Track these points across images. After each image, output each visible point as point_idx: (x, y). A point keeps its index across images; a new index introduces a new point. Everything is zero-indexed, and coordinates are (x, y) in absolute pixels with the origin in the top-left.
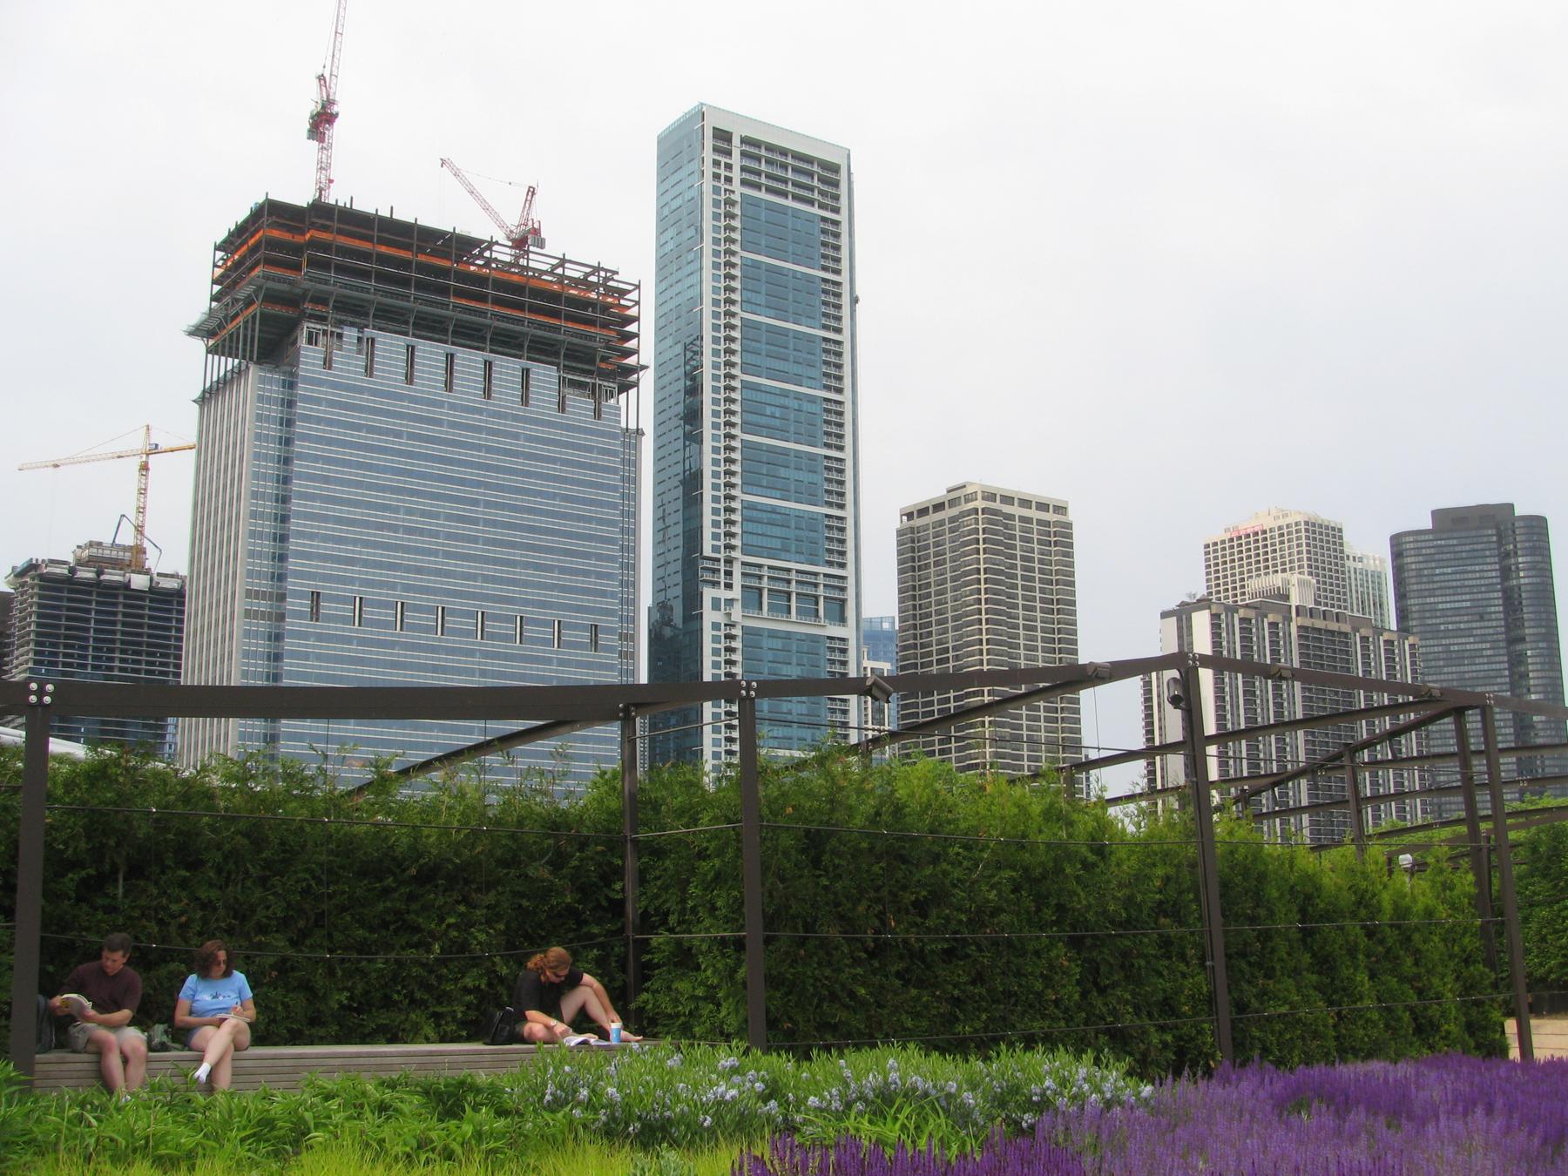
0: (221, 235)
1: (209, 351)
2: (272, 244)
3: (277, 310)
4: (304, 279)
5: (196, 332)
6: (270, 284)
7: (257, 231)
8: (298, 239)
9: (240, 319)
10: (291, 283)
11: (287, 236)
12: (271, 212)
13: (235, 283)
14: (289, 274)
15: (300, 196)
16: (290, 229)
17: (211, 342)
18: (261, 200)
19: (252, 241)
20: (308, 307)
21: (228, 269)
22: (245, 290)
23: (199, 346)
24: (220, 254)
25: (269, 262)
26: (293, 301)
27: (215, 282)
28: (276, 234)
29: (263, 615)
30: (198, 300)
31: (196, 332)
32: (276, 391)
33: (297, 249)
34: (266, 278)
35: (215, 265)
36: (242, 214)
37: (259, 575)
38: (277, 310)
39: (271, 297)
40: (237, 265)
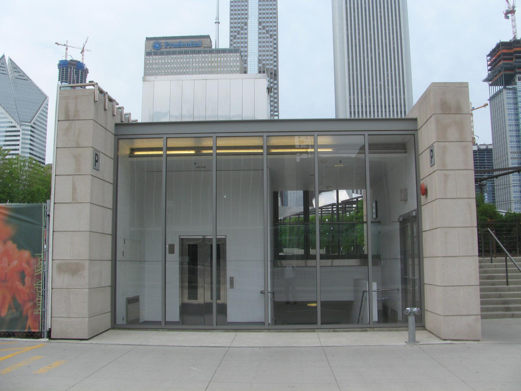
0: (488, 53)
1: (490, 85)
2: (504, 54)
3: (508, 72)
4: (514, 62)
5: (486, 80)
6: (505, 66)
7: (499, 51)
8: (511, 51)
9: (498, 77)
10: (512, 64)
11: (508, 51)
12: (501, 45)
13: (495, 65)
14: (510, 62)
15: (508, 38)
16: (508, 49)
17: (490, 83)
18: (499, 42)
19: (498, 54)
20: (517, 70)
21: (492, 62)
22: (498, 68)
23: (487, 84)
24: (489, 58)
25: (504, 59)
26: (512, 69)
27: (488, 66)
28: (505, 51)
29: (516, 158)
30: (485, 73)
31: (486, 80)
32: (511, 95)
33: (511, 54)
34: (504, 64)
35: (488, 61)
36: (494, 46)
37: (514, 147)
38: (508, 72)
39: (506, 69)
40: (495, 61)
